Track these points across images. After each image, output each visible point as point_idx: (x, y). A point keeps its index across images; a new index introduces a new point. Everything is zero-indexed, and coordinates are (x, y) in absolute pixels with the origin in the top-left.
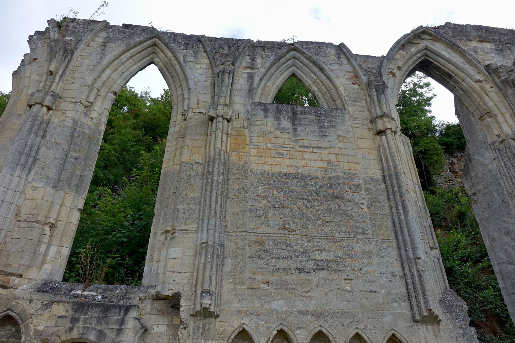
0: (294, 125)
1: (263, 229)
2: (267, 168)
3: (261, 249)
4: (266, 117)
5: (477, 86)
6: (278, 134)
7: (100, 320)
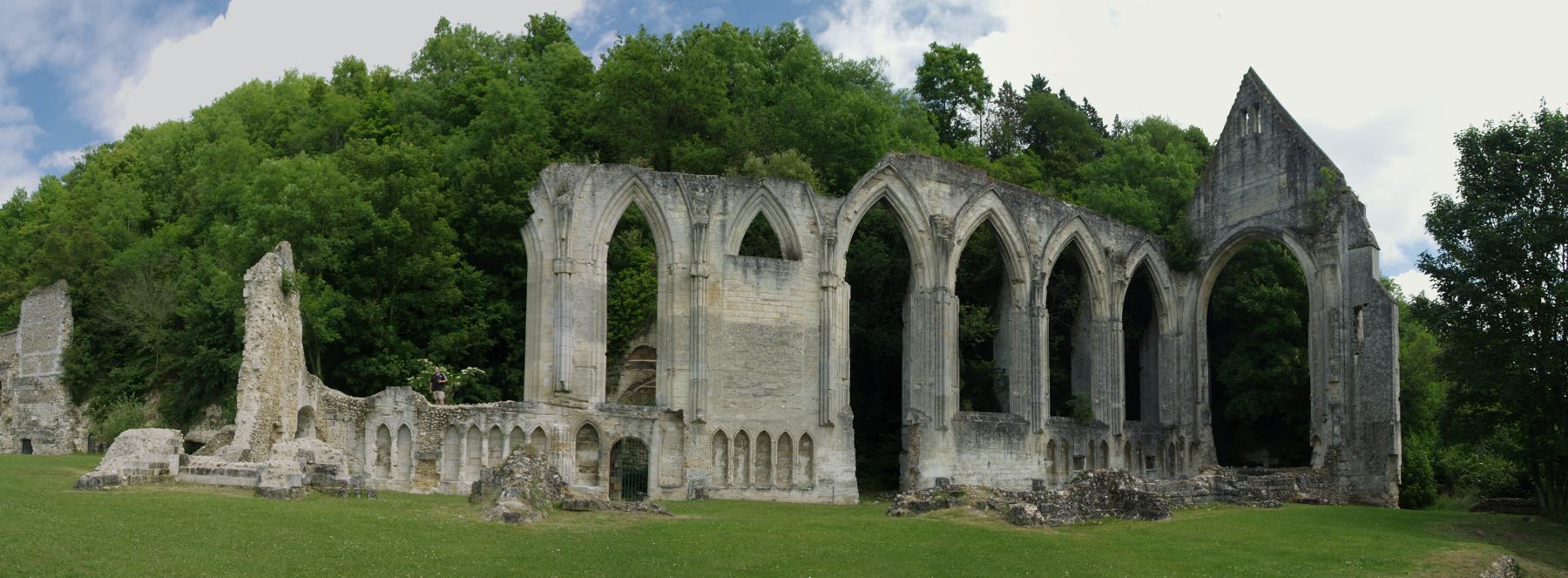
1: (732, 368)
2: (735, 319)
3: (731, 381)
5: (918, 235)
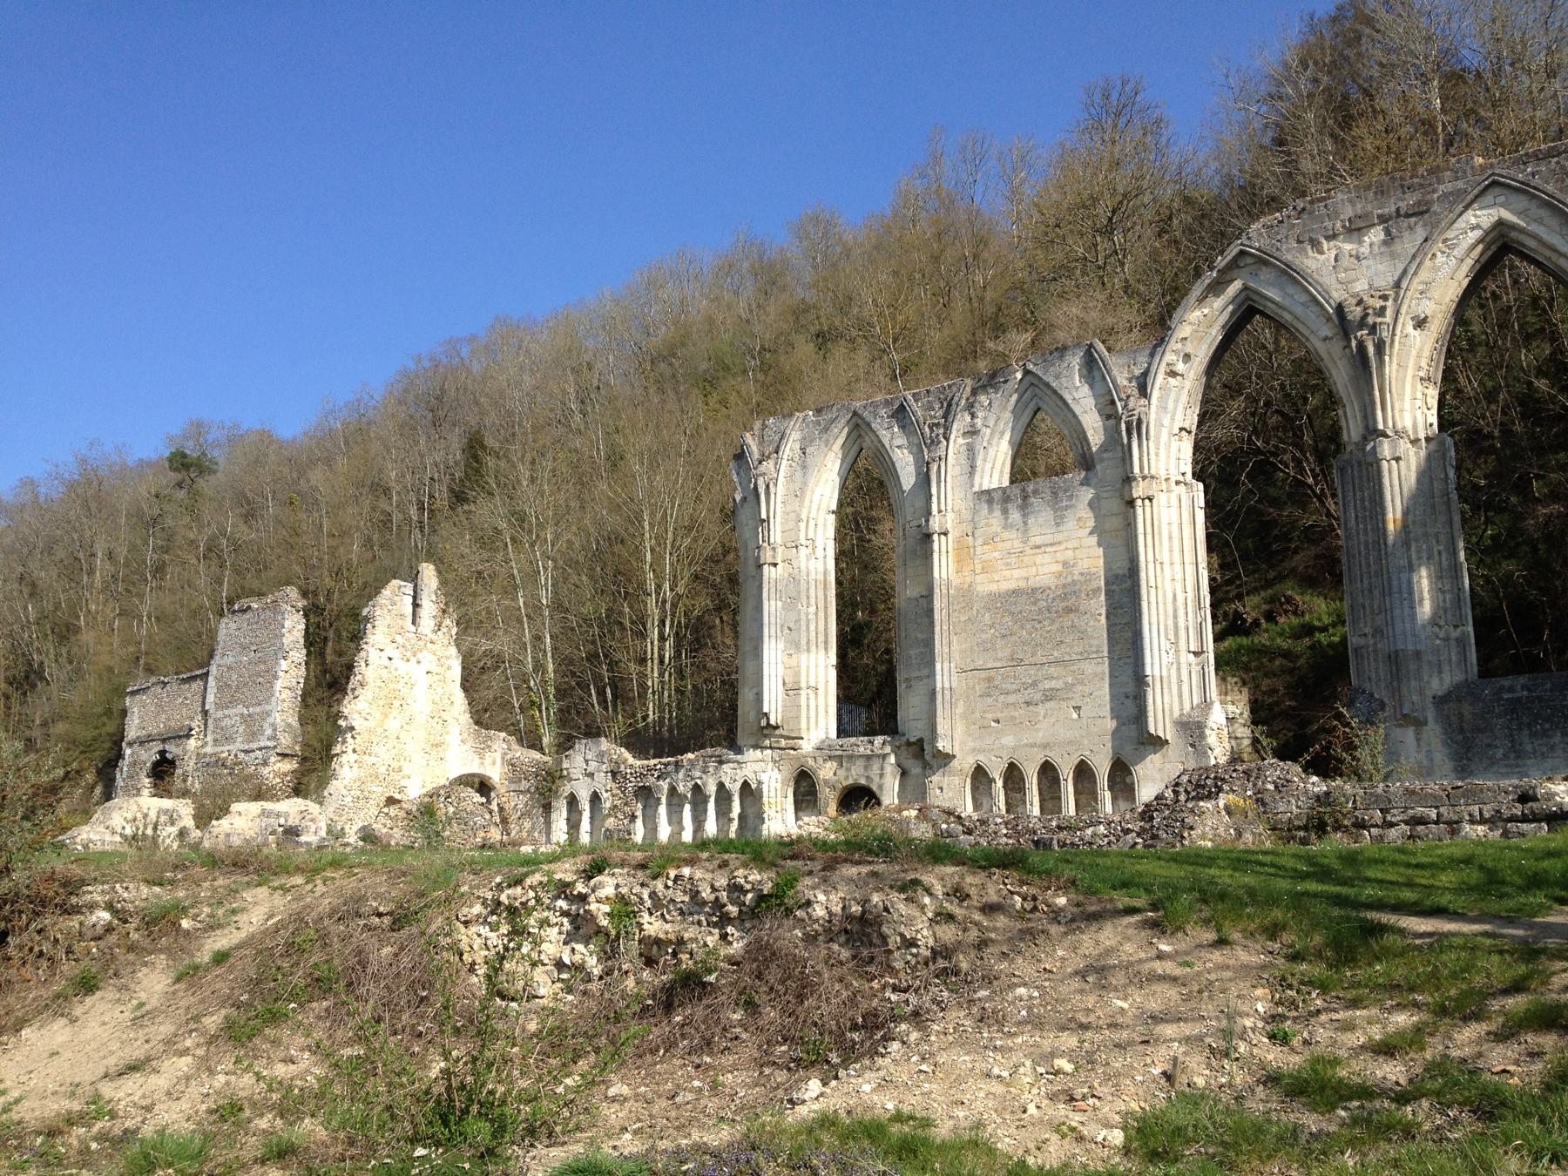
0: (1024, 516)
2: (994, 587)
4: (991, 511)
6: (1006, 535)
7: (866, 768)
